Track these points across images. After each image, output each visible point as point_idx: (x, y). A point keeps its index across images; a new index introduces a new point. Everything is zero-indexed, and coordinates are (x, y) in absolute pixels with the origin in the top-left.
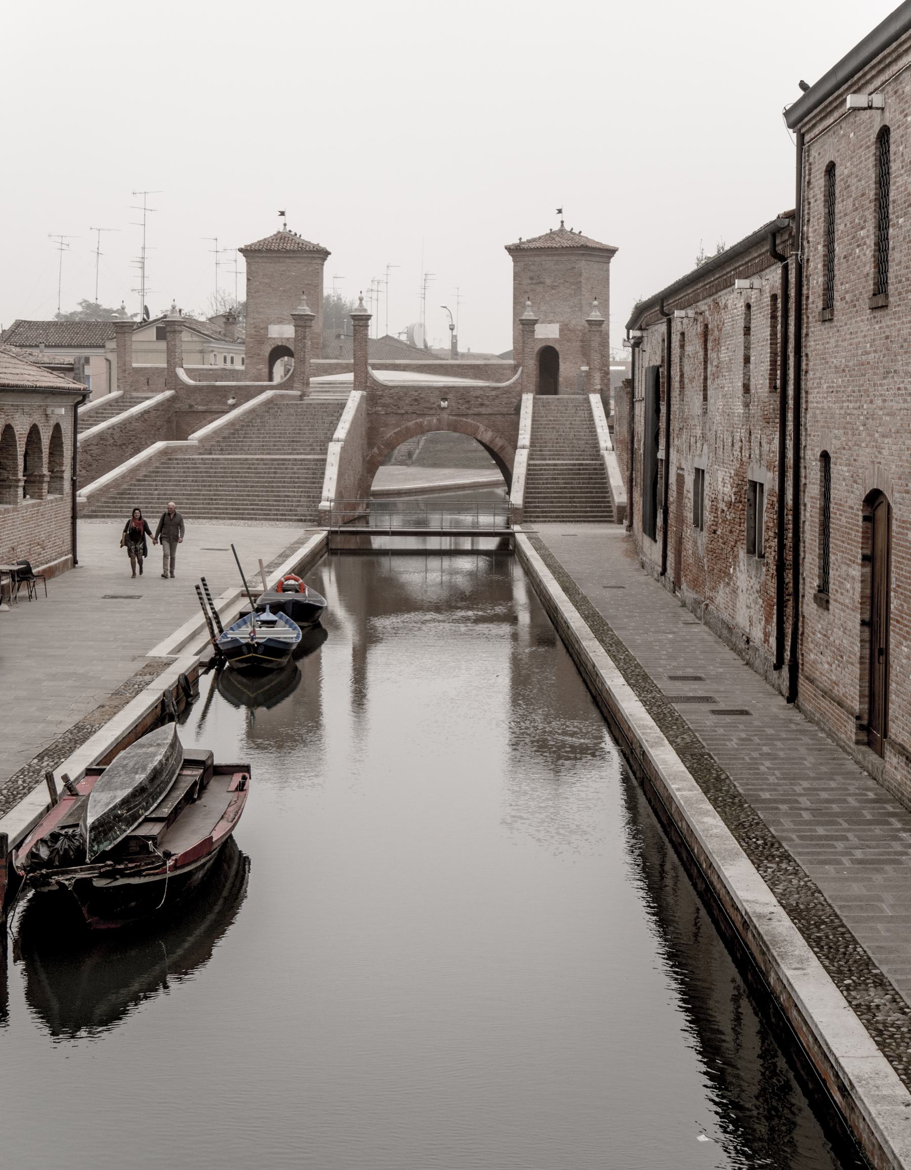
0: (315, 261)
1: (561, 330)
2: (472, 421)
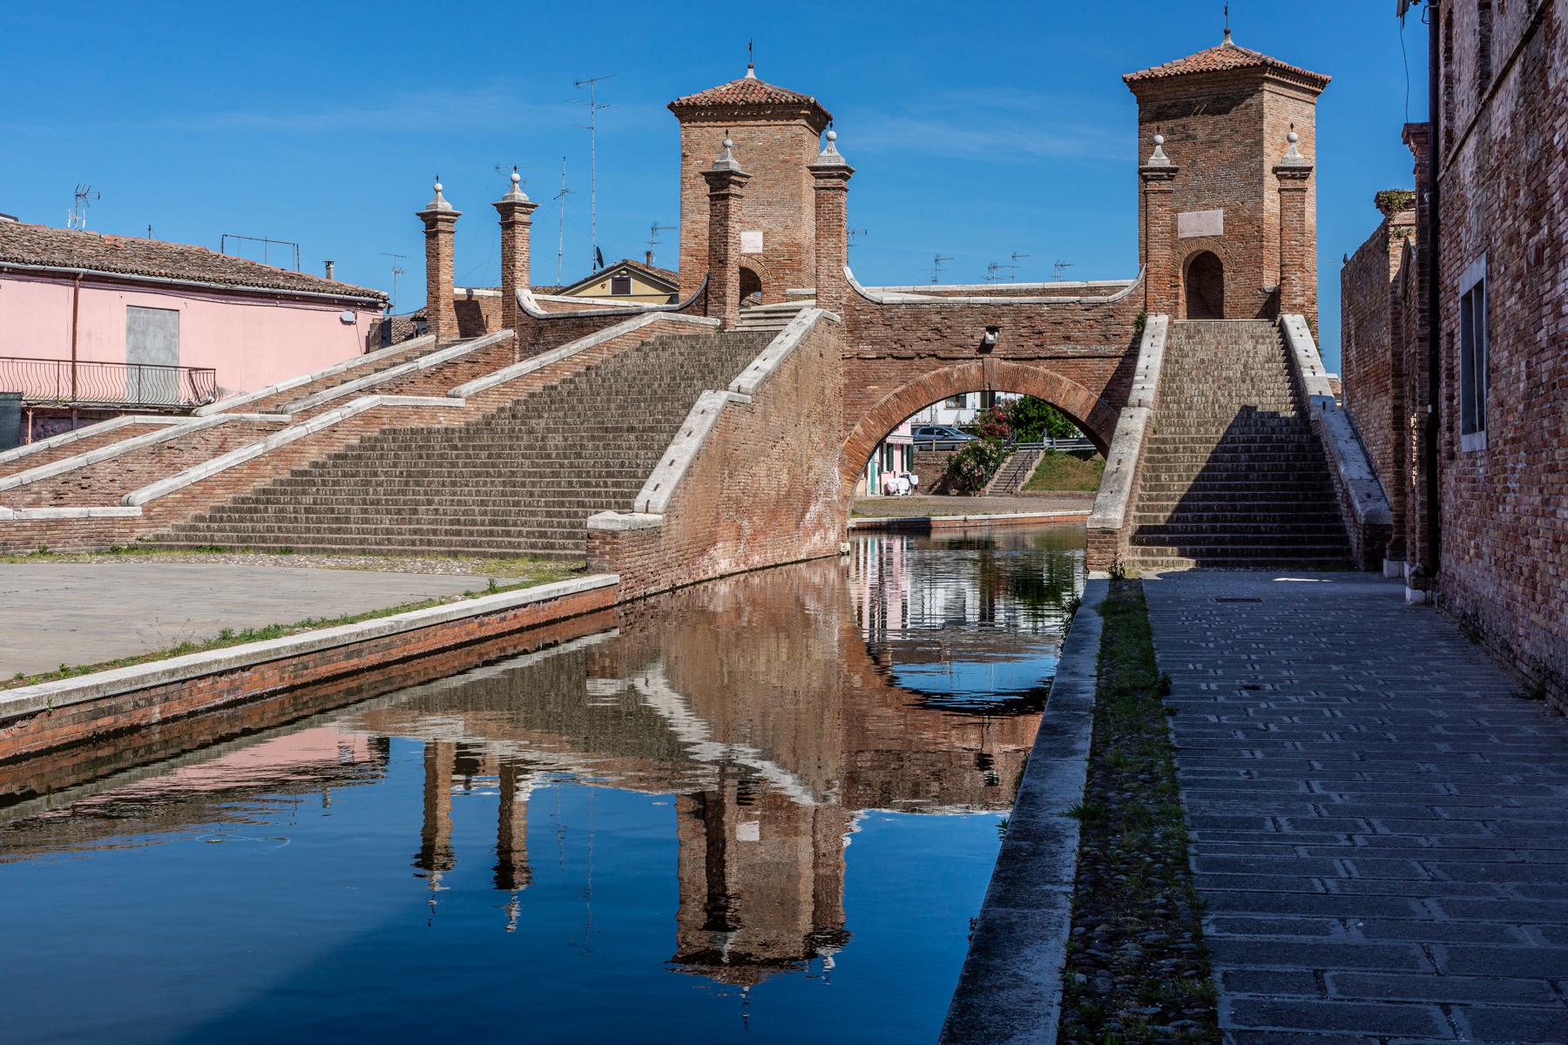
2: (1047, 371)
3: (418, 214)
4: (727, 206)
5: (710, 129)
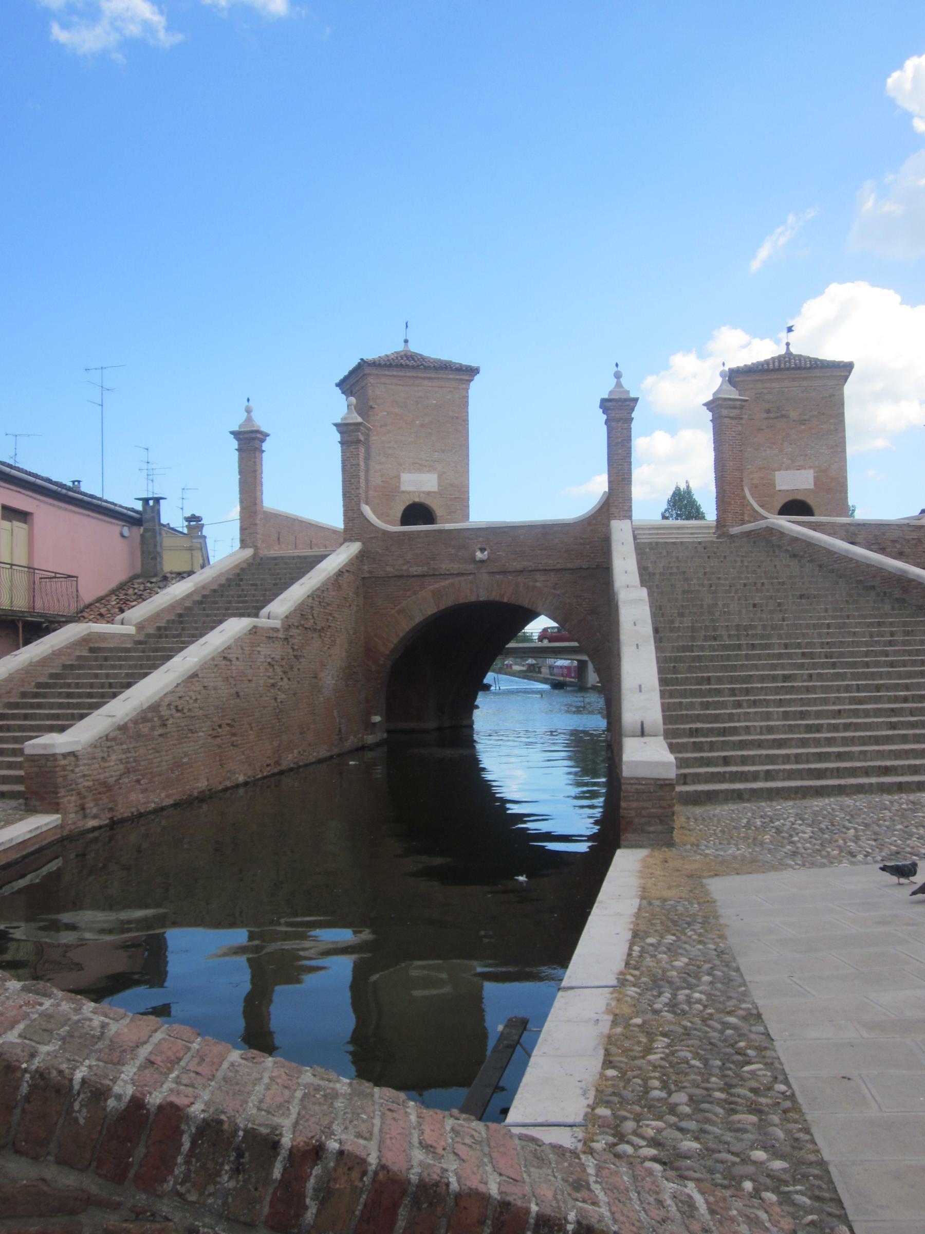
0: (464, 386)
1: (816, 479)
3: (232, 433)
4: (629, 429)
5: (393, 387)
